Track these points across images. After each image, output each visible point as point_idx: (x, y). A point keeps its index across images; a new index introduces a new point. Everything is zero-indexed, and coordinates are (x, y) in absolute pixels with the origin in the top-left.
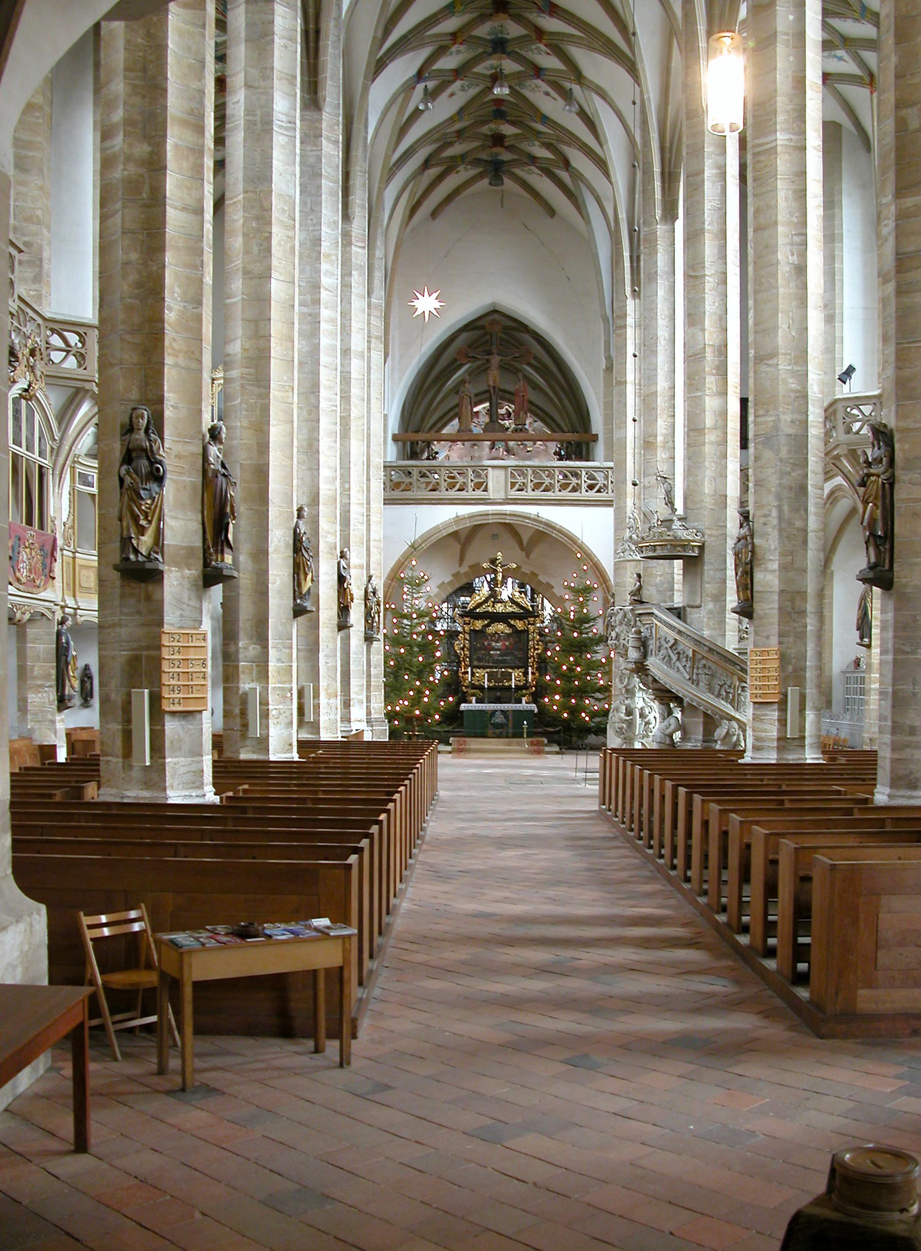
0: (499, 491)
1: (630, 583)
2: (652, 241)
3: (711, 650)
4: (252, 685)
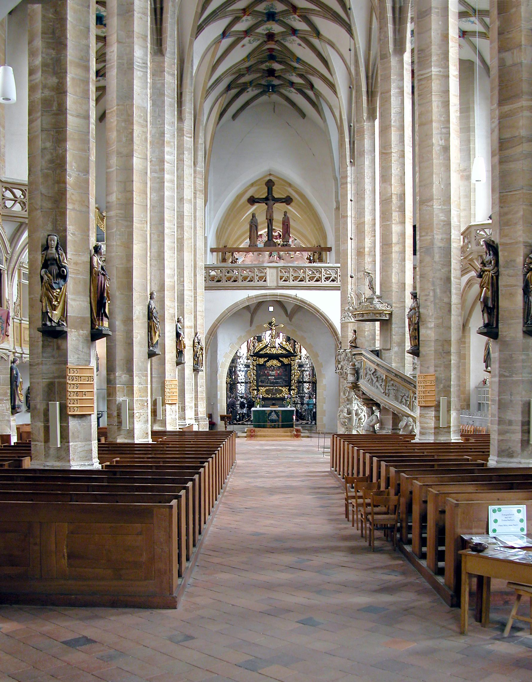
0: (273, 282)
1: (350, 336)
2: (361, 132)
3: (396, 375)
4: (124, 398)
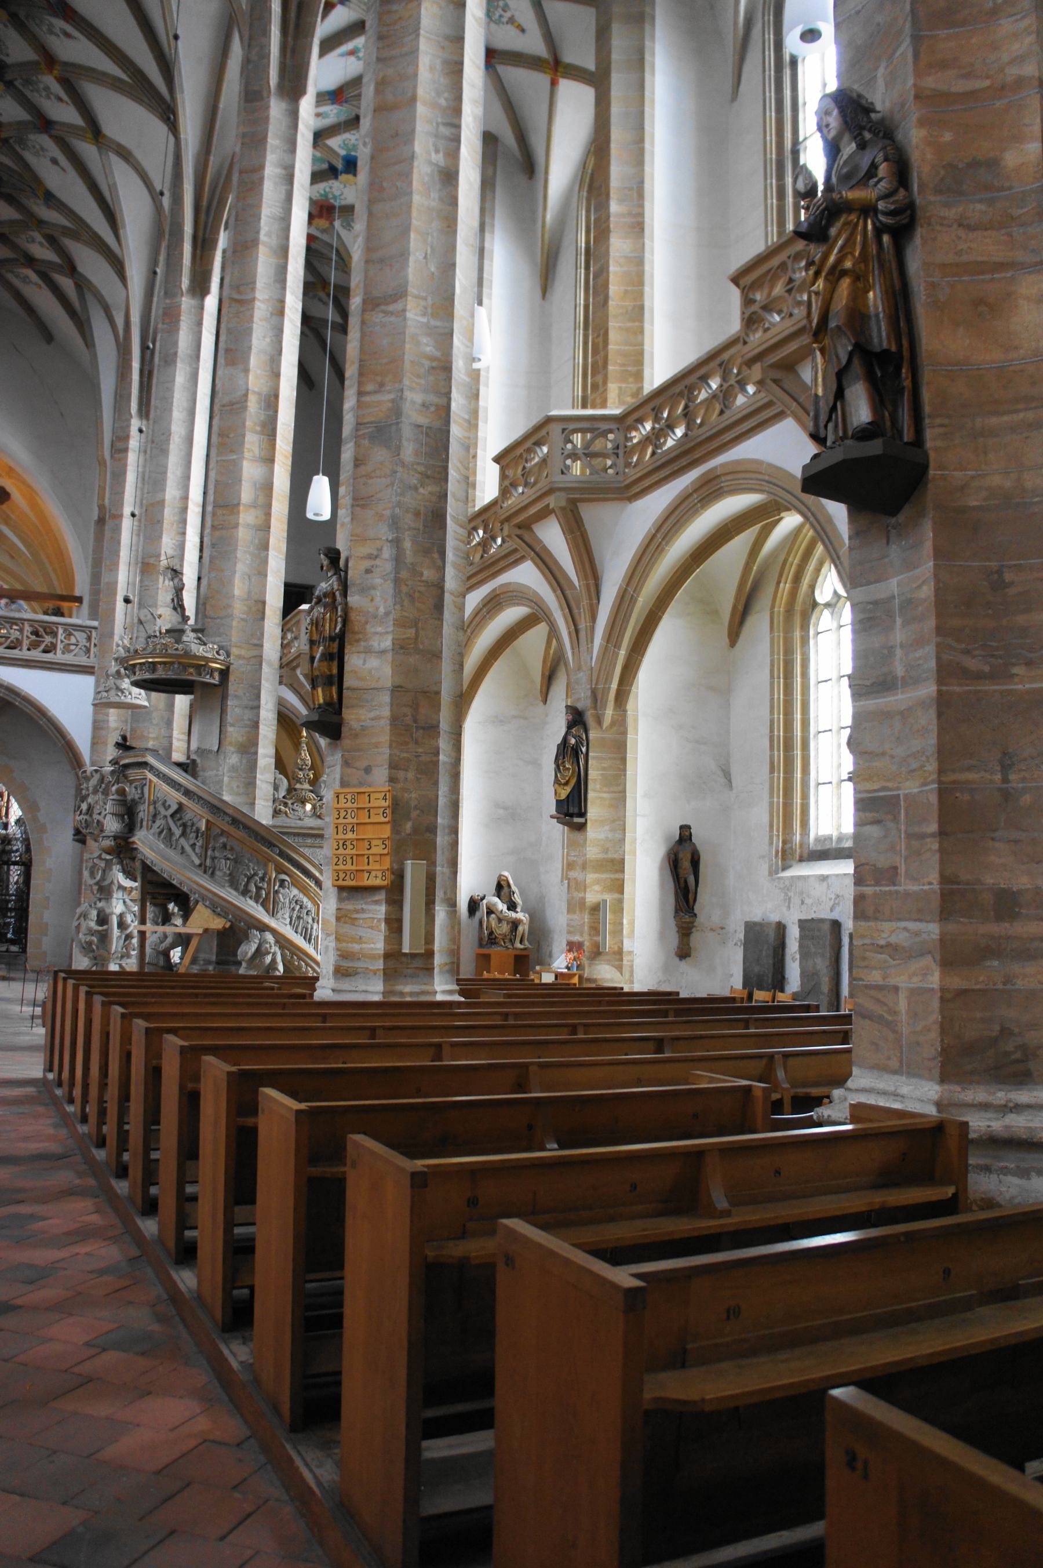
2: (172, 316)
3: (235, 822)
